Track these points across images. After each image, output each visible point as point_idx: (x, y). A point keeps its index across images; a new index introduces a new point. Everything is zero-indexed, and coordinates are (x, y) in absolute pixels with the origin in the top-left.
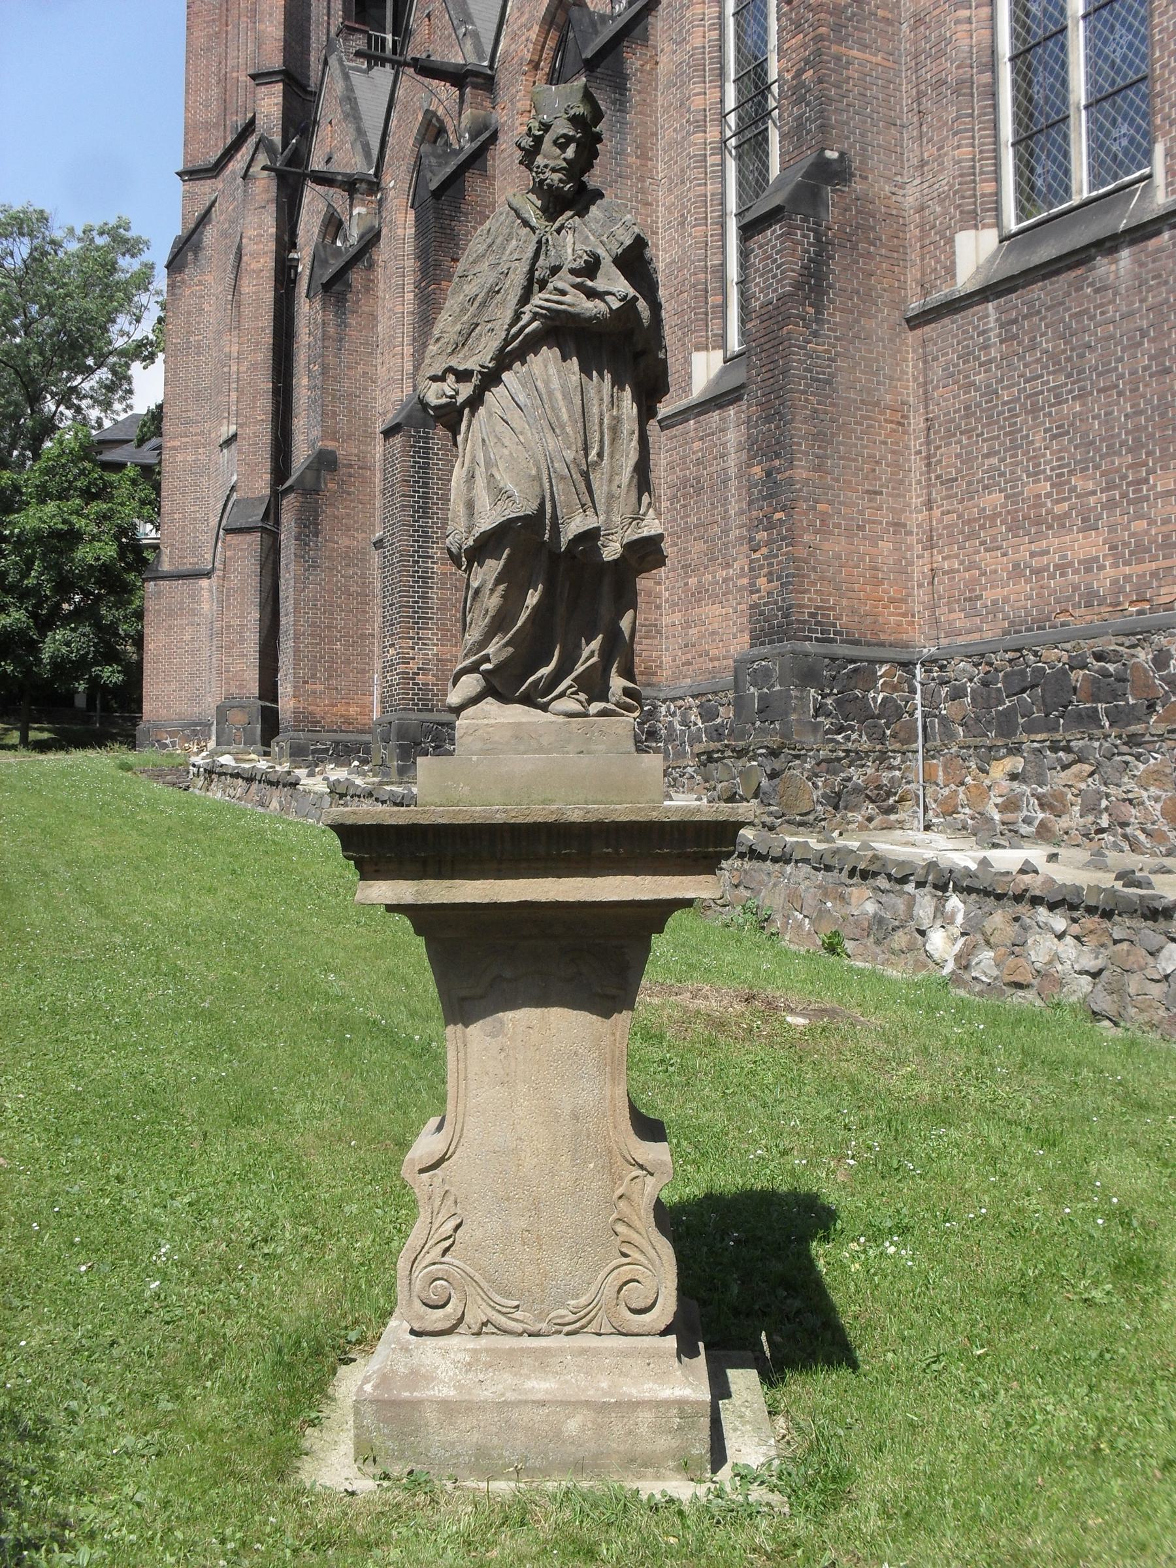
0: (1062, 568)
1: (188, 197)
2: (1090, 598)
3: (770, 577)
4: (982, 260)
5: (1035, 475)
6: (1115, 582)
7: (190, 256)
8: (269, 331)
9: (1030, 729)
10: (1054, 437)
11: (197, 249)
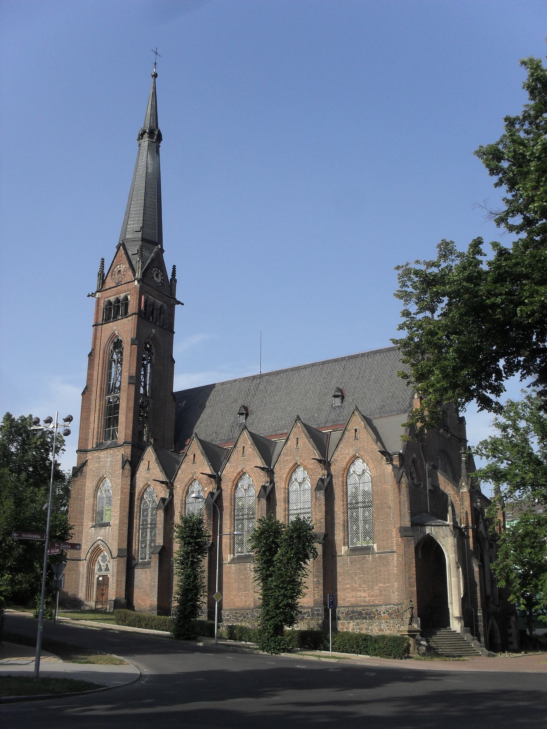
0: (360, 597)
1: (79, 458)
2: (365, 602)
7: (79, 474)
8: (128, 508)
9: (356, 619)
11: (82, 472)
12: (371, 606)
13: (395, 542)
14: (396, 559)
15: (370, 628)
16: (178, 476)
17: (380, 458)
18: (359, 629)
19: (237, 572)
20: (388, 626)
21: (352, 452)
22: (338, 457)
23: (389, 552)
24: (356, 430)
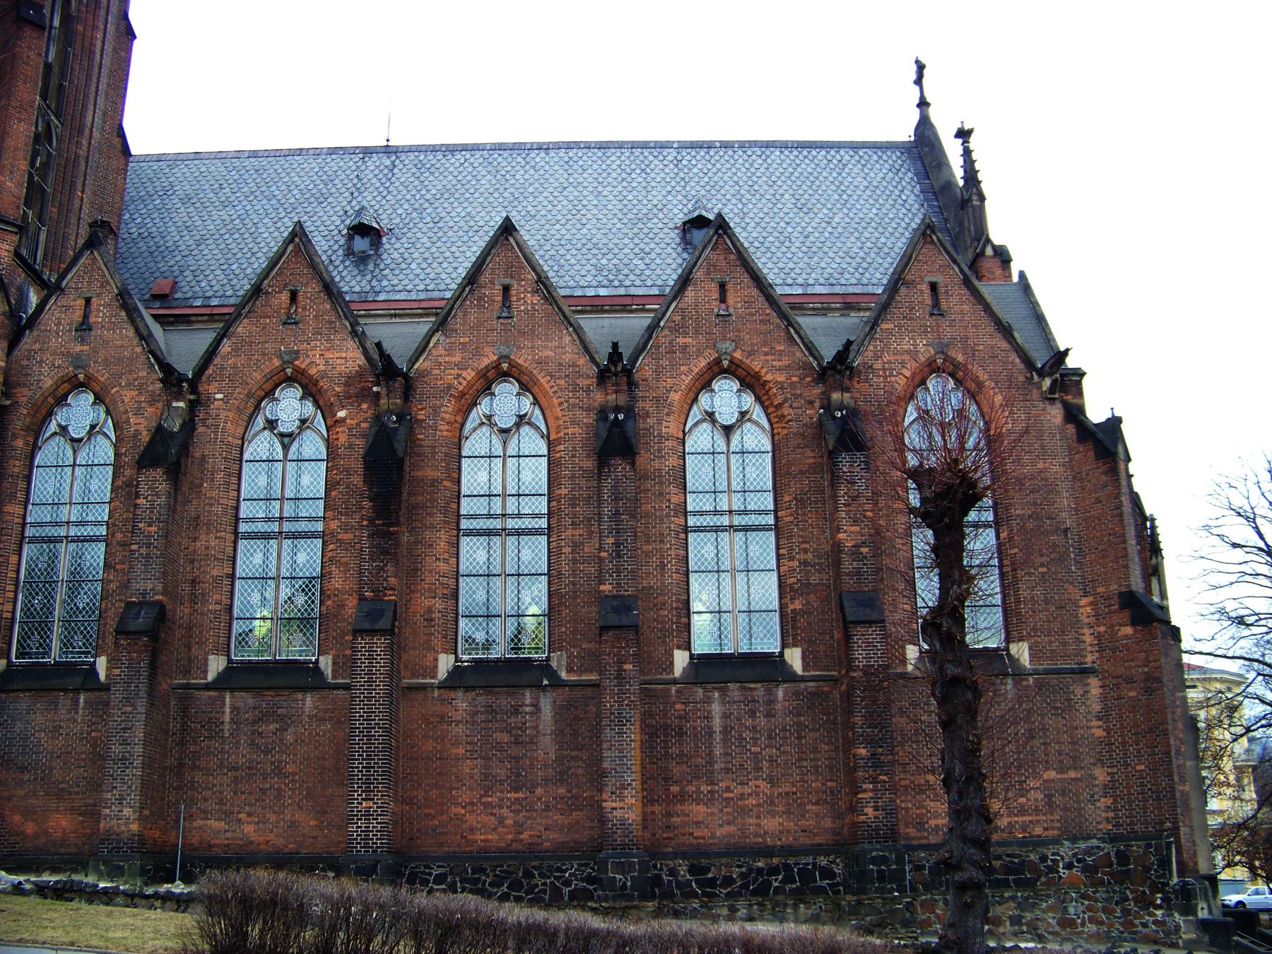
3: (876, 808)
6: (1010, 823)
12: (1022, 843)
13: (1088, 639)
15: (1028, 916)
16: (217, 360)
17: (1021, 378)
19: (479, 718)
20: (1089, 909)
21: (924, 349)
23: (1072, 671)
24: (933, 287)
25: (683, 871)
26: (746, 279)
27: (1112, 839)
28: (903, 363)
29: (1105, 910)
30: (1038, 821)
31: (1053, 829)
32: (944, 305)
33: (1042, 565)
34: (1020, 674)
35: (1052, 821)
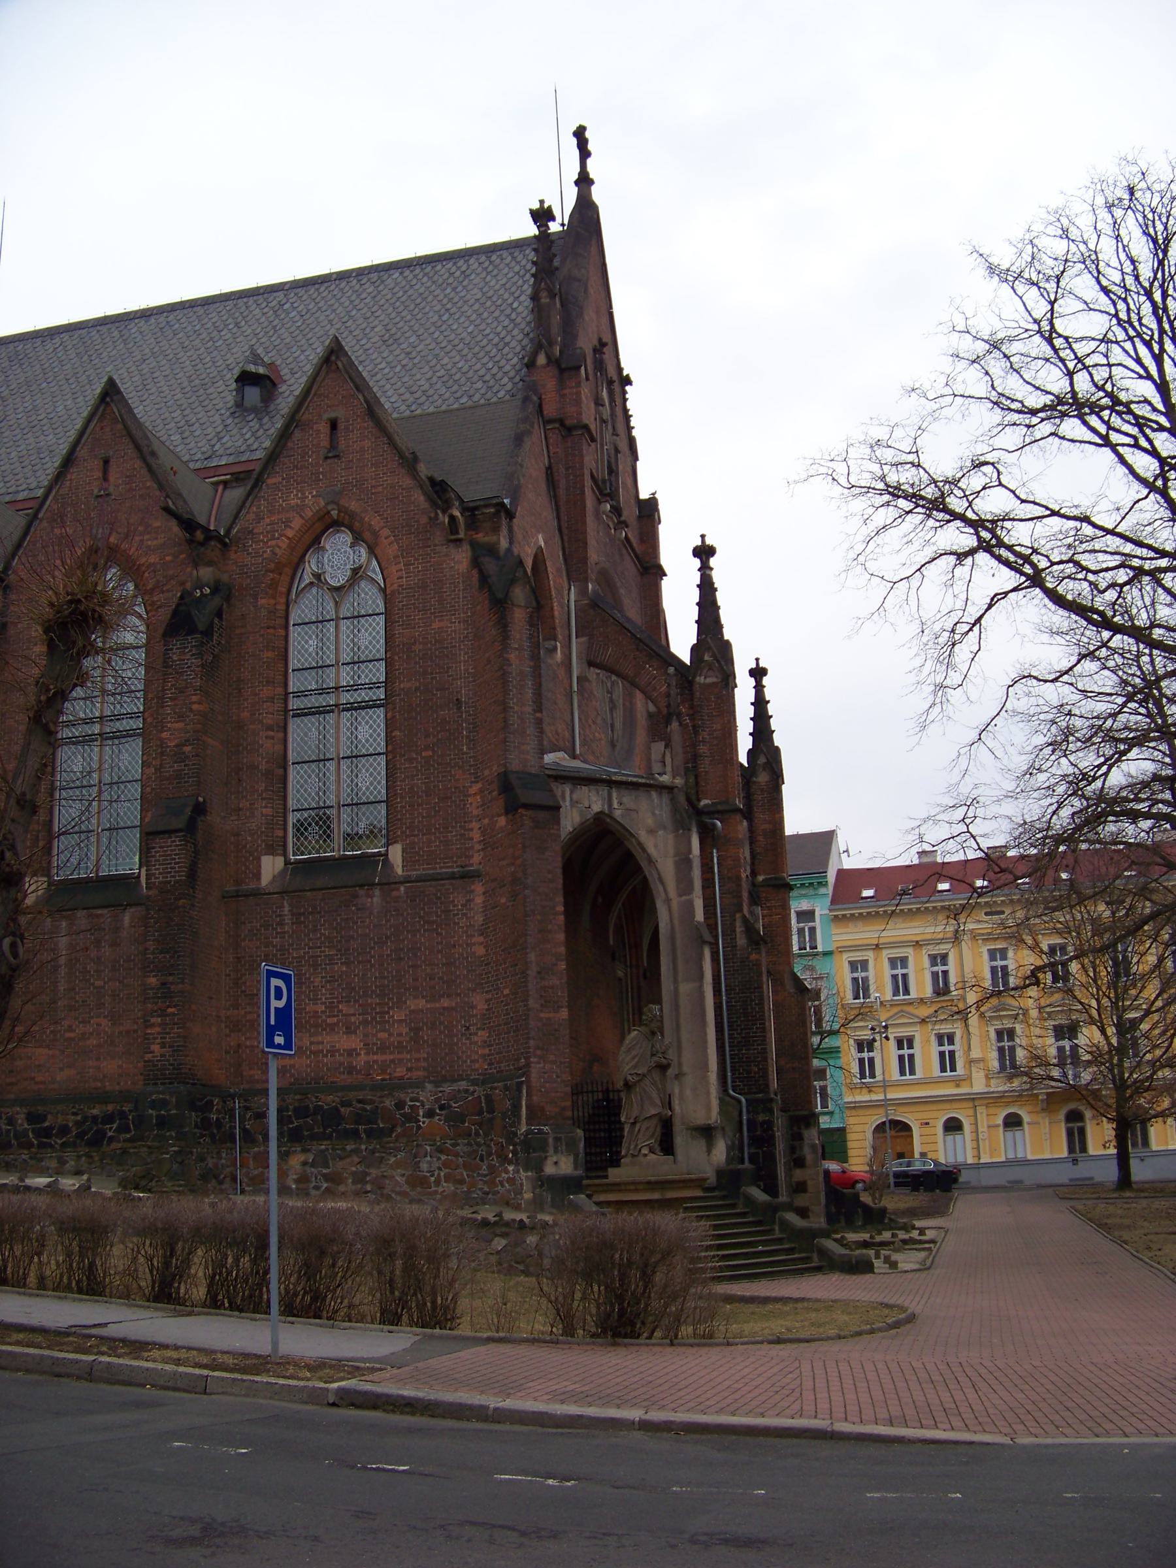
0: (332, 1052)
2: (351, 1070)
3: (163, 1045)
4: (276, 872)
5: (315, 1000)
6: (367, 1062)
9: (314, 1137)
10: (329, 982)
12: (377, 1087)
13: (476, 835)
14: (479, 900)
15: (374, 1172)
17: (424, 520)
18: (326, 1177)
20: (446, 1165)
21: (314, 502)
22: (259, 519)
23: (452, 877)
24: (334, 425)
25: (21, 1120)
26: (131, 451)
27: (487, 1079)
28: (287, 523)
29: (465, 1166)
30: (401, 1060)
31: (418, 1069)
32: (342, 445)
33: (427, 748)
34: (389, 884)
35: (418, 1060)
